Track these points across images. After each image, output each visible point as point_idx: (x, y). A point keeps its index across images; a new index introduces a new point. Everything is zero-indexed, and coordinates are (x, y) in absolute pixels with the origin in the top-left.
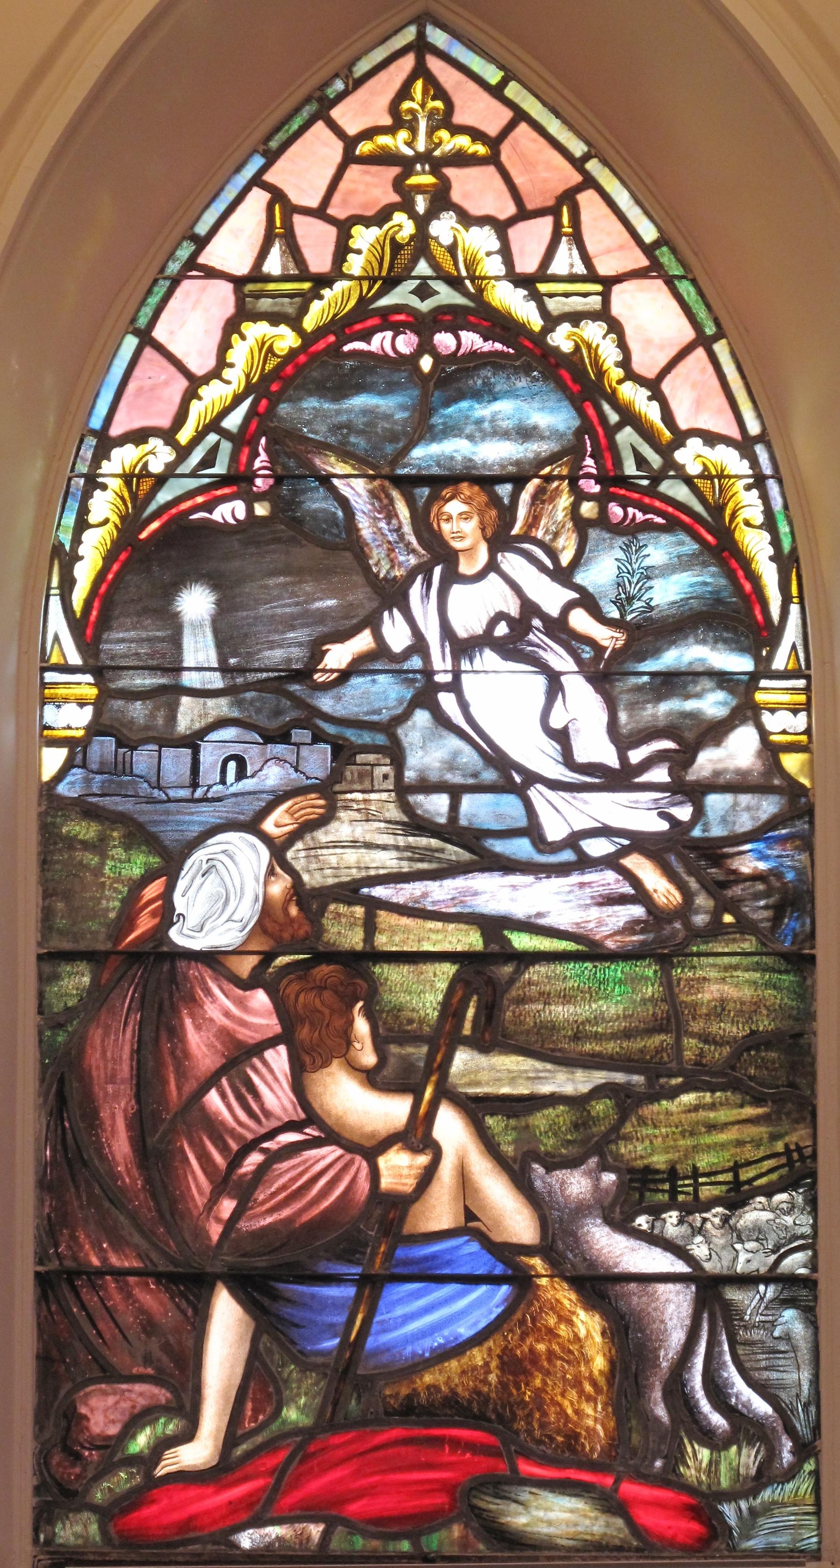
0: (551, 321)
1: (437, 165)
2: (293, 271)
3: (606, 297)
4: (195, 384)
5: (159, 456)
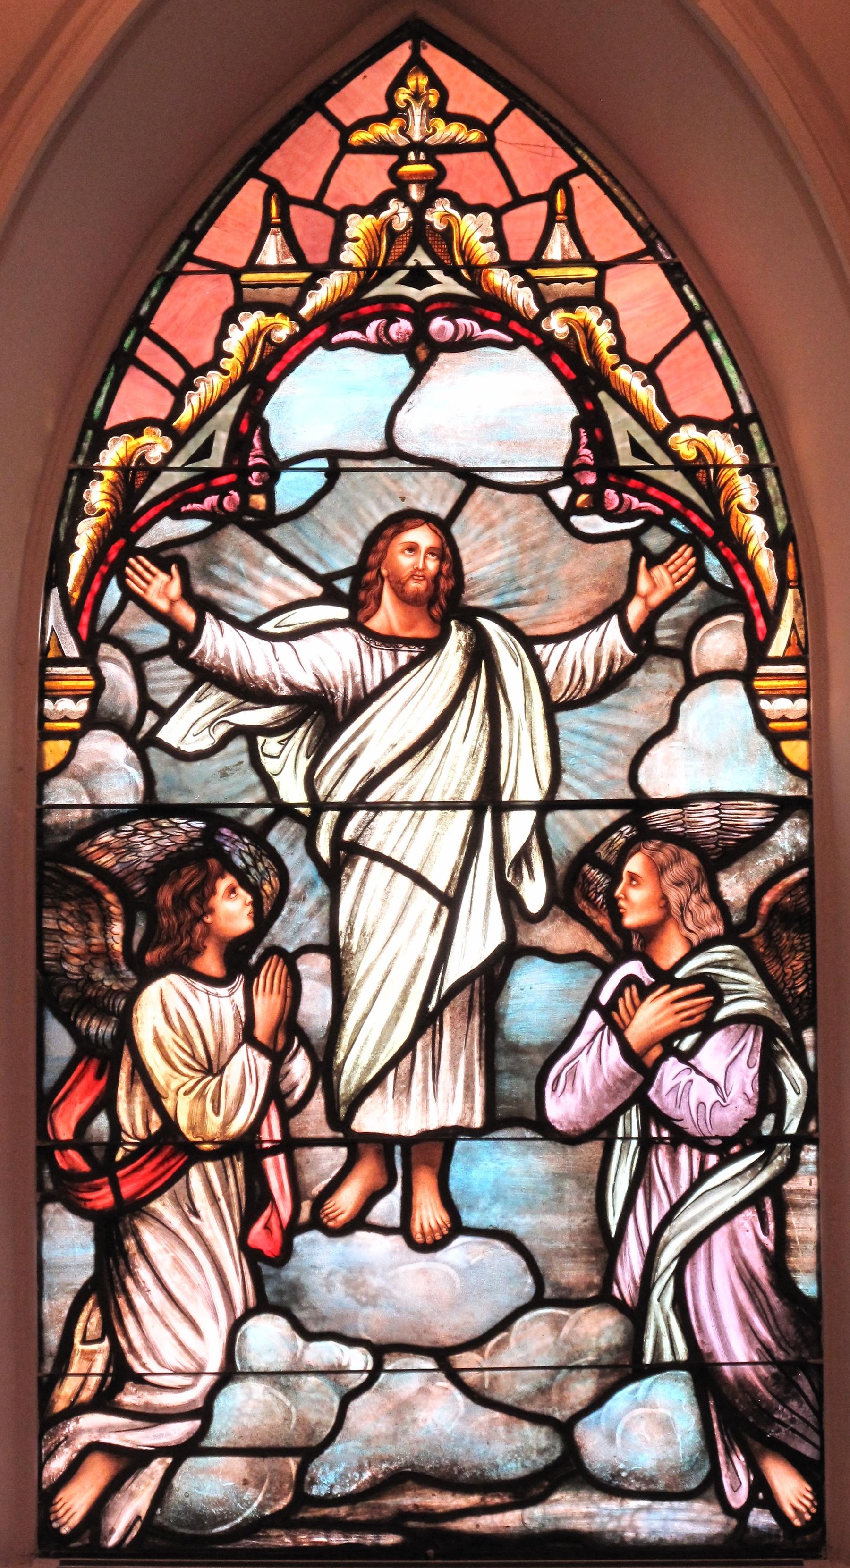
0: (546, 309)
1: (431, 152)
2: (292, 261)
3: (600, 282)
5: (156, 445)
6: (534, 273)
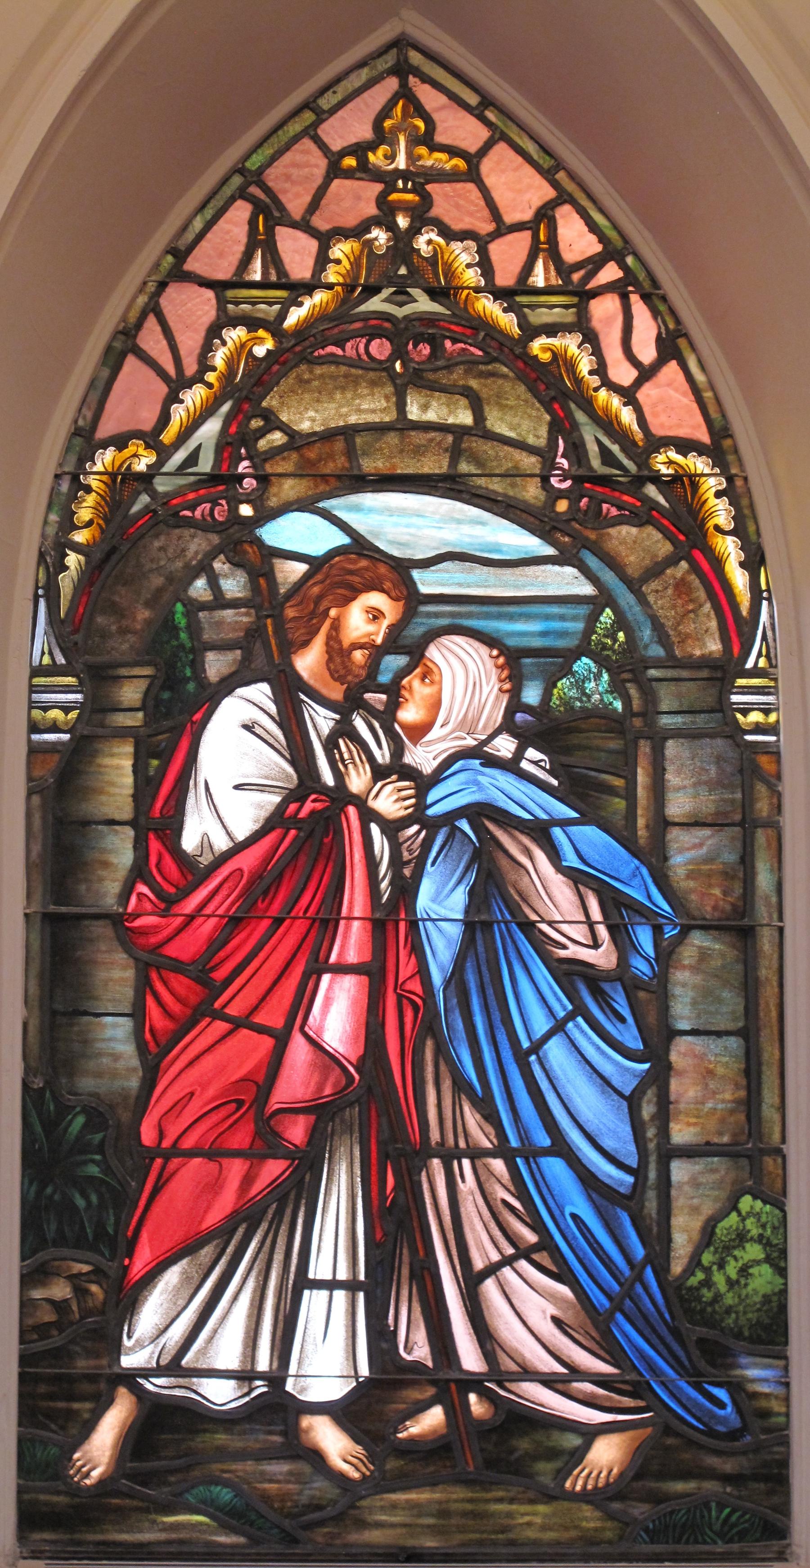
0: (530, 332)
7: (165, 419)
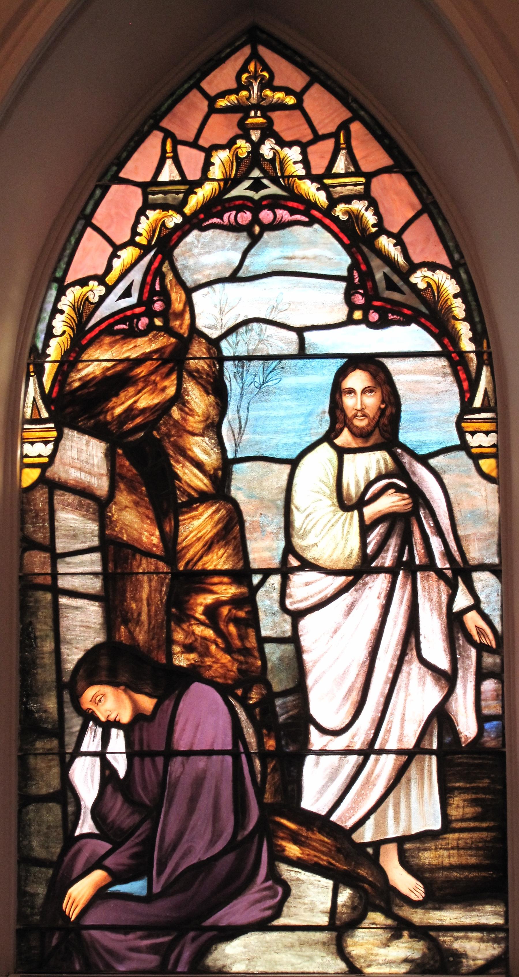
0: (333, 202)
3: (367, 185)
4: (117, 248)
6: (328, 181)
7: (109, 268)
